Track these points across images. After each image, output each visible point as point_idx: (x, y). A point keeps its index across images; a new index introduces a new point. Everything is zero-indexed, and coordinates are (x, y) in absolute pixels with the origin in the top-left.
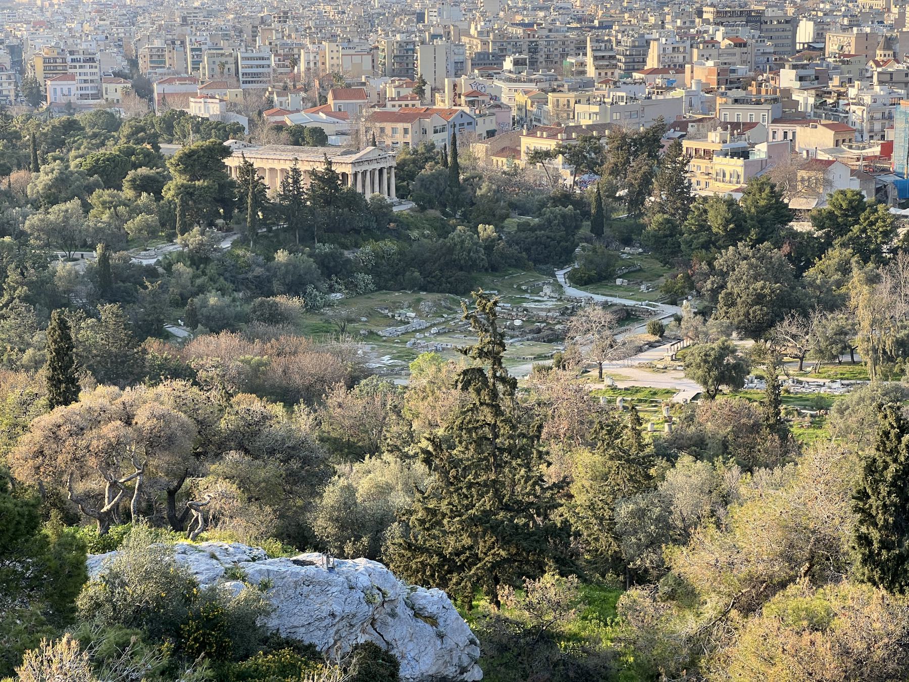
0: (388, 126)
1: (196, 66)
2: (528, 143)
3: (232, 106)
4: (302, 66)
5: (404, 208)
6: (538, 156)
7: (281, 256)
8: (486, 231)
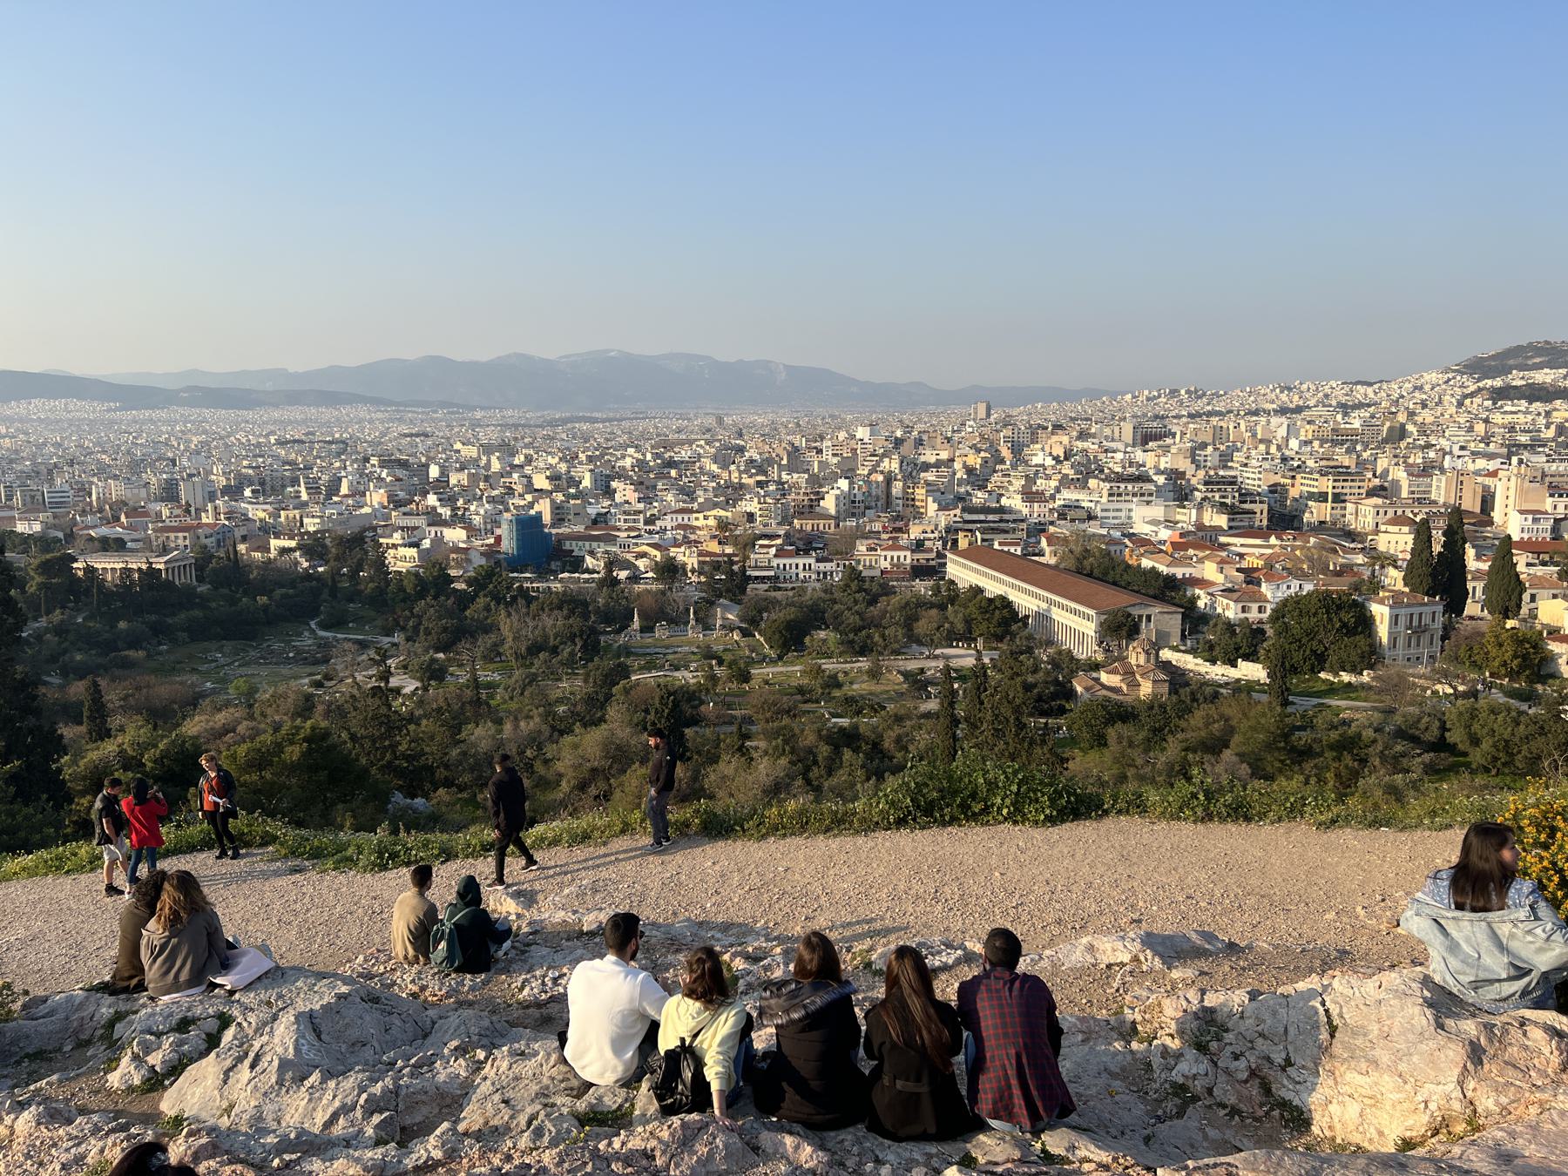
0: (172, 535)
1: (9, 498)
2: (275, 543)
5: (203, 588)
6: (284, 551)
7: (122, 625)
8: (262, 600)
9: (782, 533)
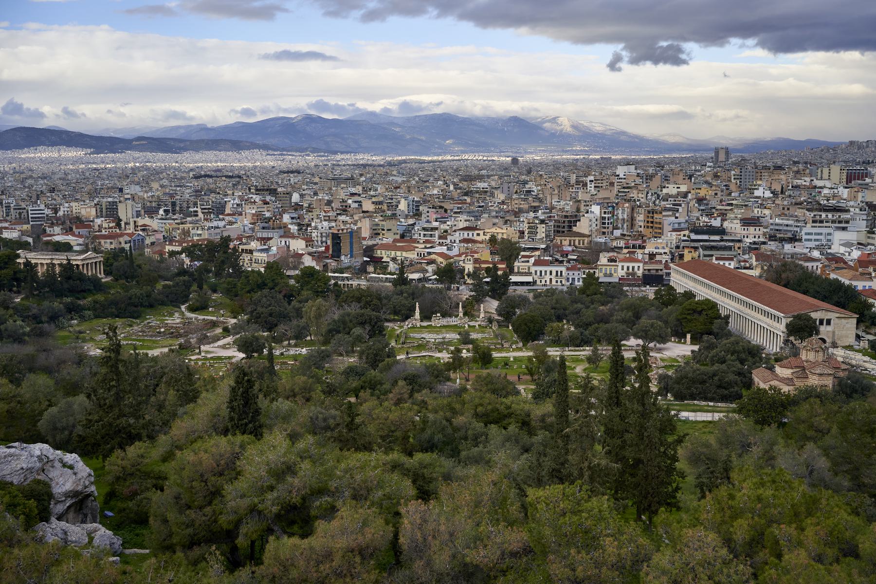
0: (102, 241)
3: (23, 233)
4: (61, 213)
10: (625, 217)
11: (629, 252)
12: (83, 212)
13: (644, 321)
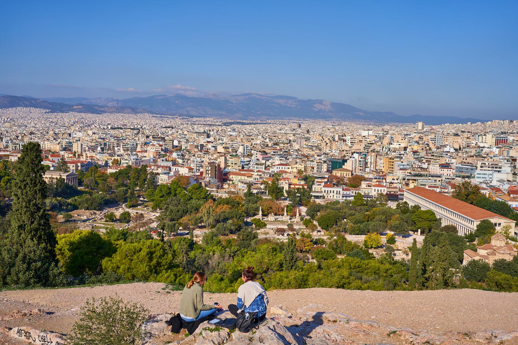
9: (327, 176)
10: (372, 161)
11: (377, 181)
12: (52, 147)
13: (394, 222)
